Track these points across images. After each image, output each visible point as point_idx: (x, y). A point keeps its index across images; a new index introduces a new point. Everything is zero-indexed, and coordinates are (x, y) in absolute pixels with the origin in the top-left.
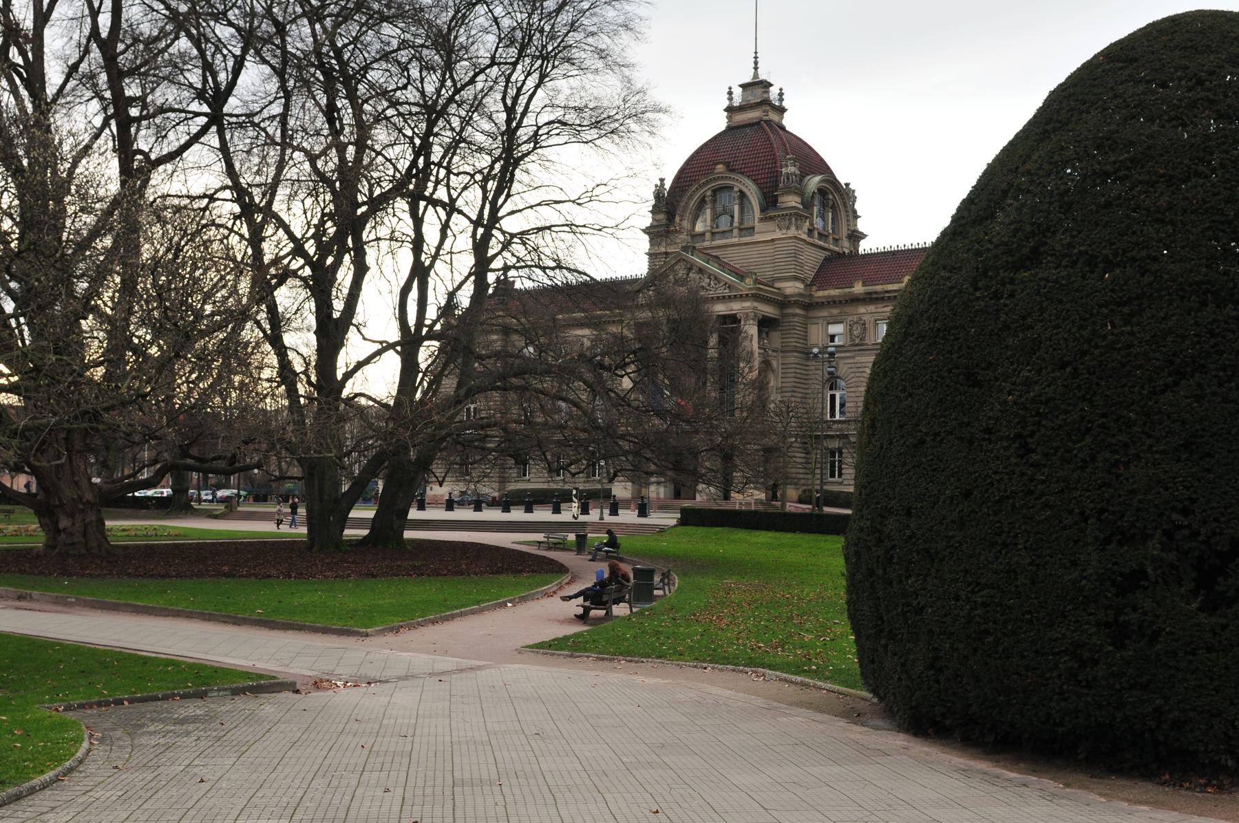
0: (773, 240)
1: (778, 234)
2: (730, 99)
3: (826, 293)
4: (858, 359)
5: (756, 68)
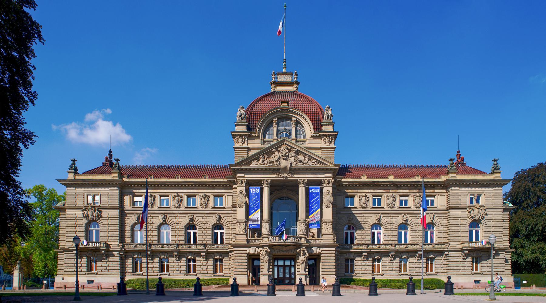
0: (321, 148)
1: (325, 145)
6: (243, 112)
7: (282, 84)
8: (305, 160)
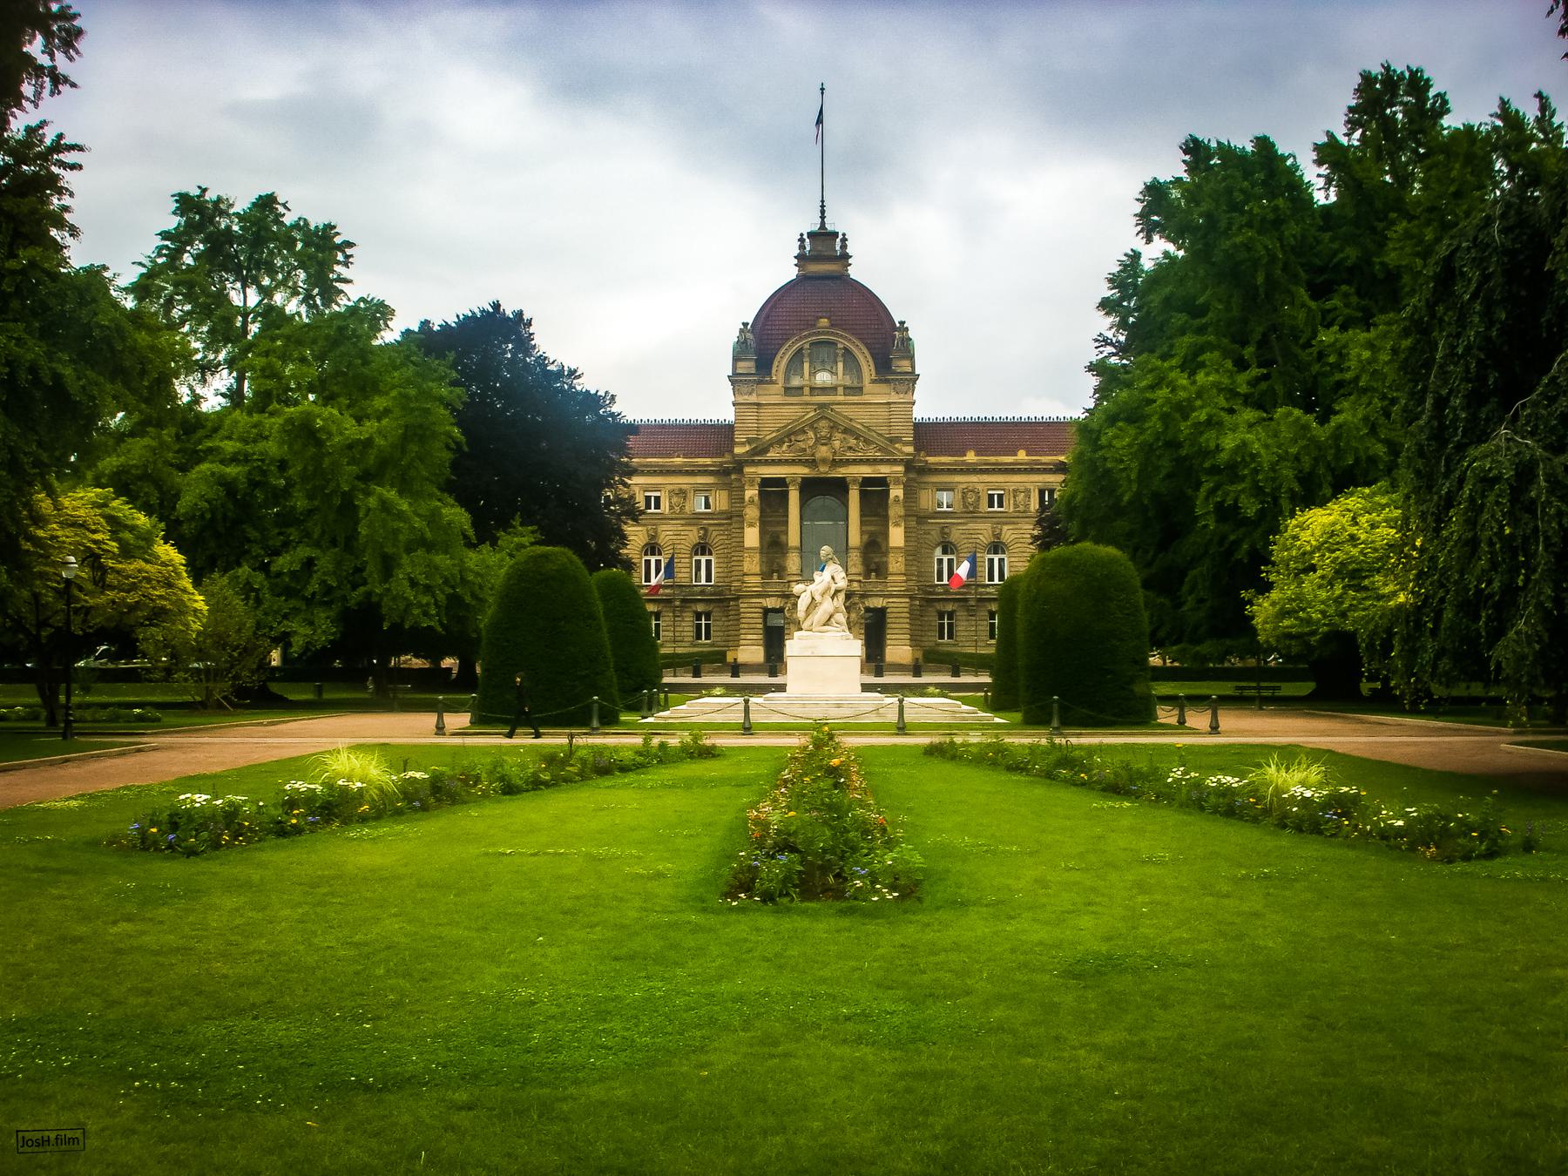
1: (894, 398)
2: (802, 247)
4: (971, 526)
5: (823, 217)
6: (749, 335)
7: (816, 258)
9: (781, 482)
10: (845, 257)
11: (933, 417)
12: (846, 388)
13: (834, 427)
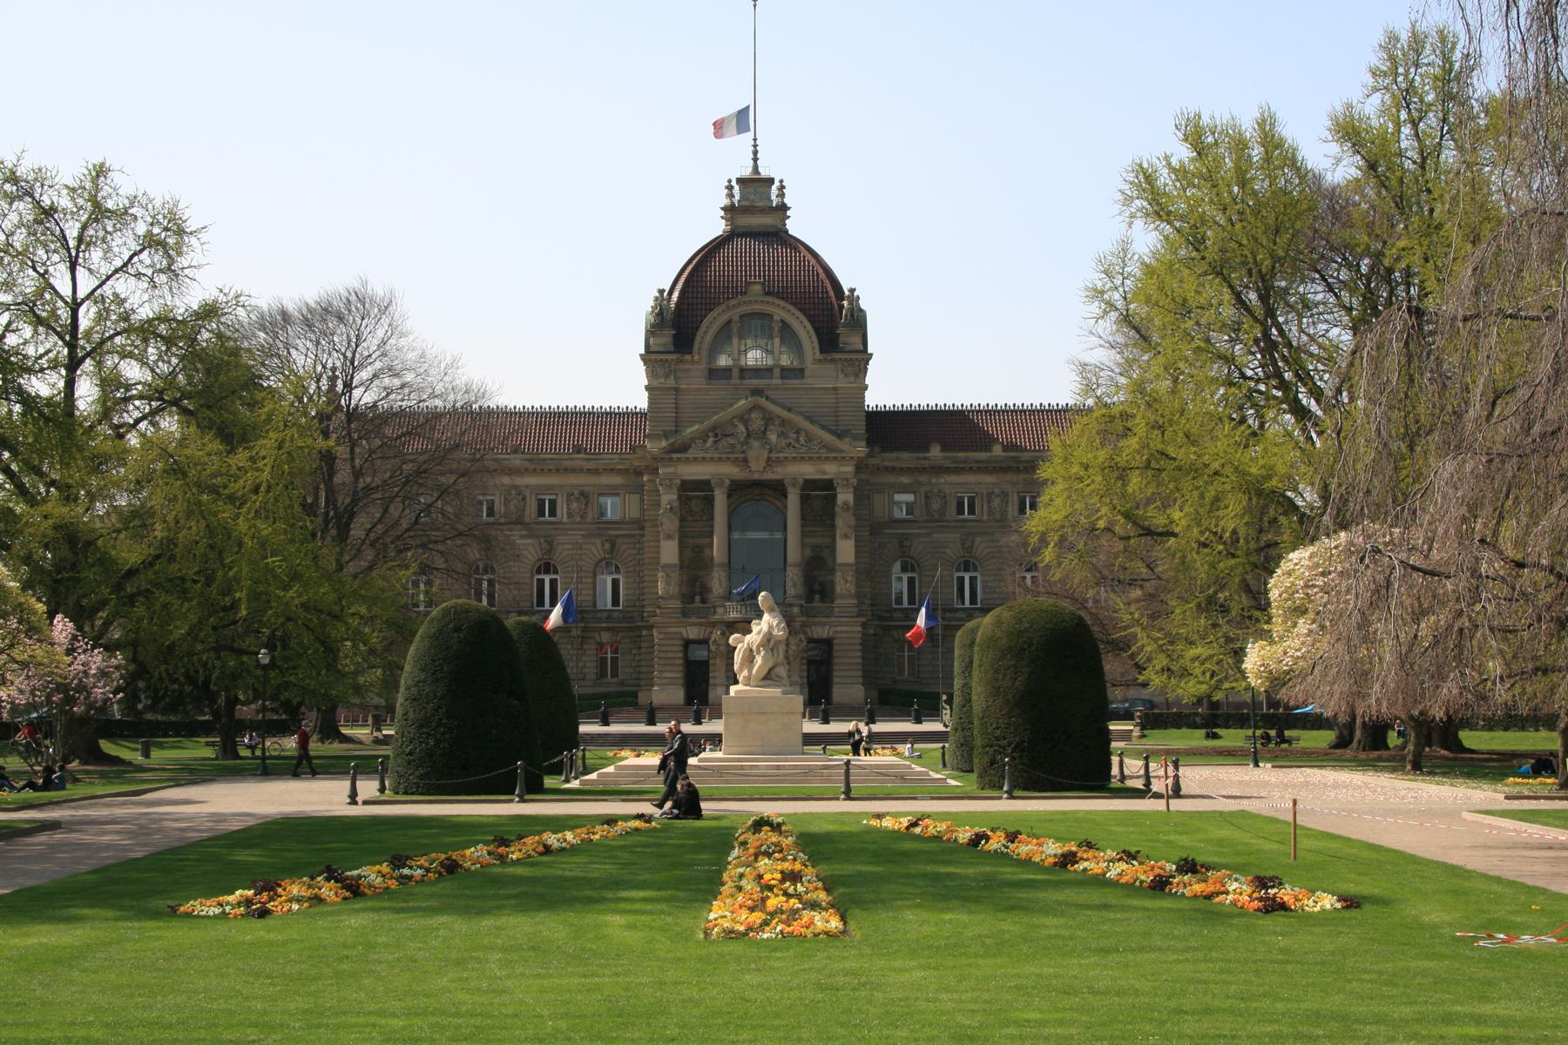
0: (835, 389)
2: (731, 196)
3: (895, 455)
5: (755, 160)
8: (797, 440)
9: (704, 486)
10: (784, 208)
11: (889, 405)
12: (783, 369)
13: (769, 419)
